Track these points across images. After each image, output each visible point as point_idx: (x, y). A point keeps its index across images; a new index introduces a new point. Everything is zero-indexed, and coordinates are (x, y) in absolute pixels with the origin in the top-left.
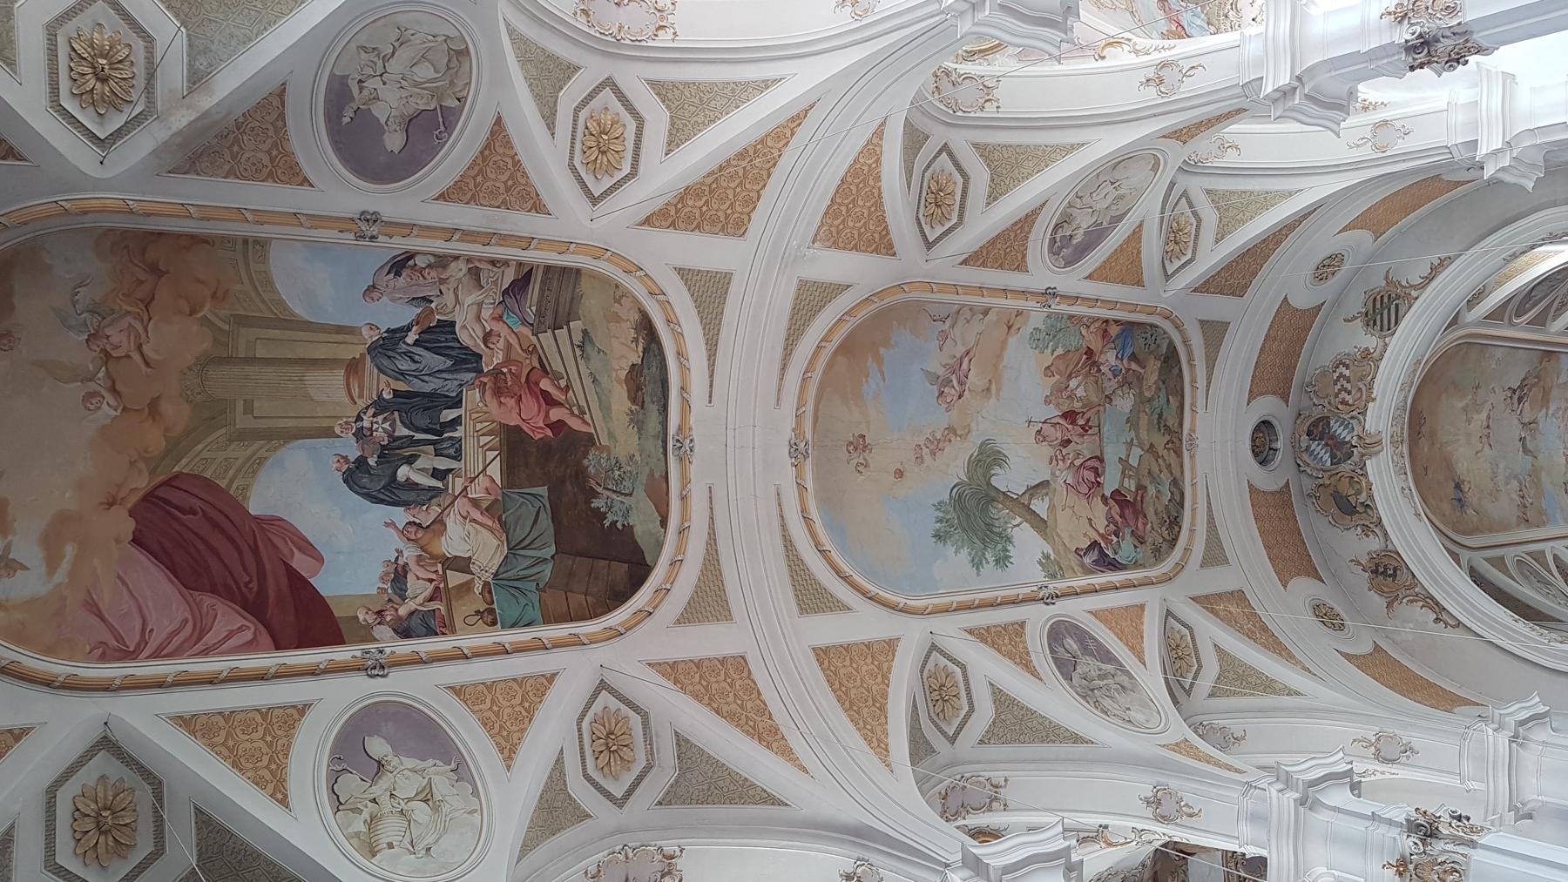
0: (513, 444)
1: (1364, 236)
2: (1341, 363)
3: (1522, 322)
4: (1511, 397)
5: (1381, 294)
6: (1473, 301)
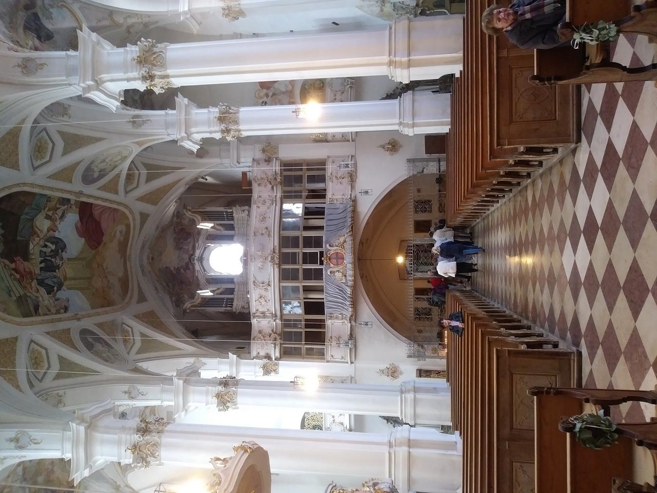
0: (26, 257)
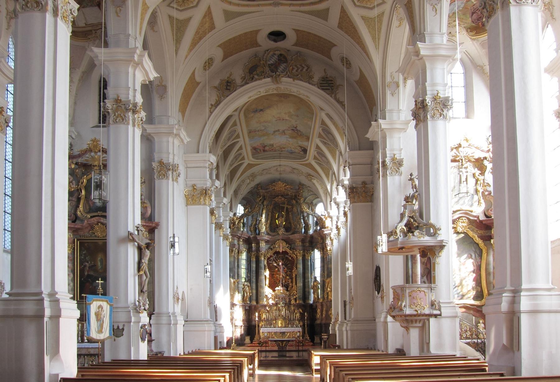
4: (293, 127)
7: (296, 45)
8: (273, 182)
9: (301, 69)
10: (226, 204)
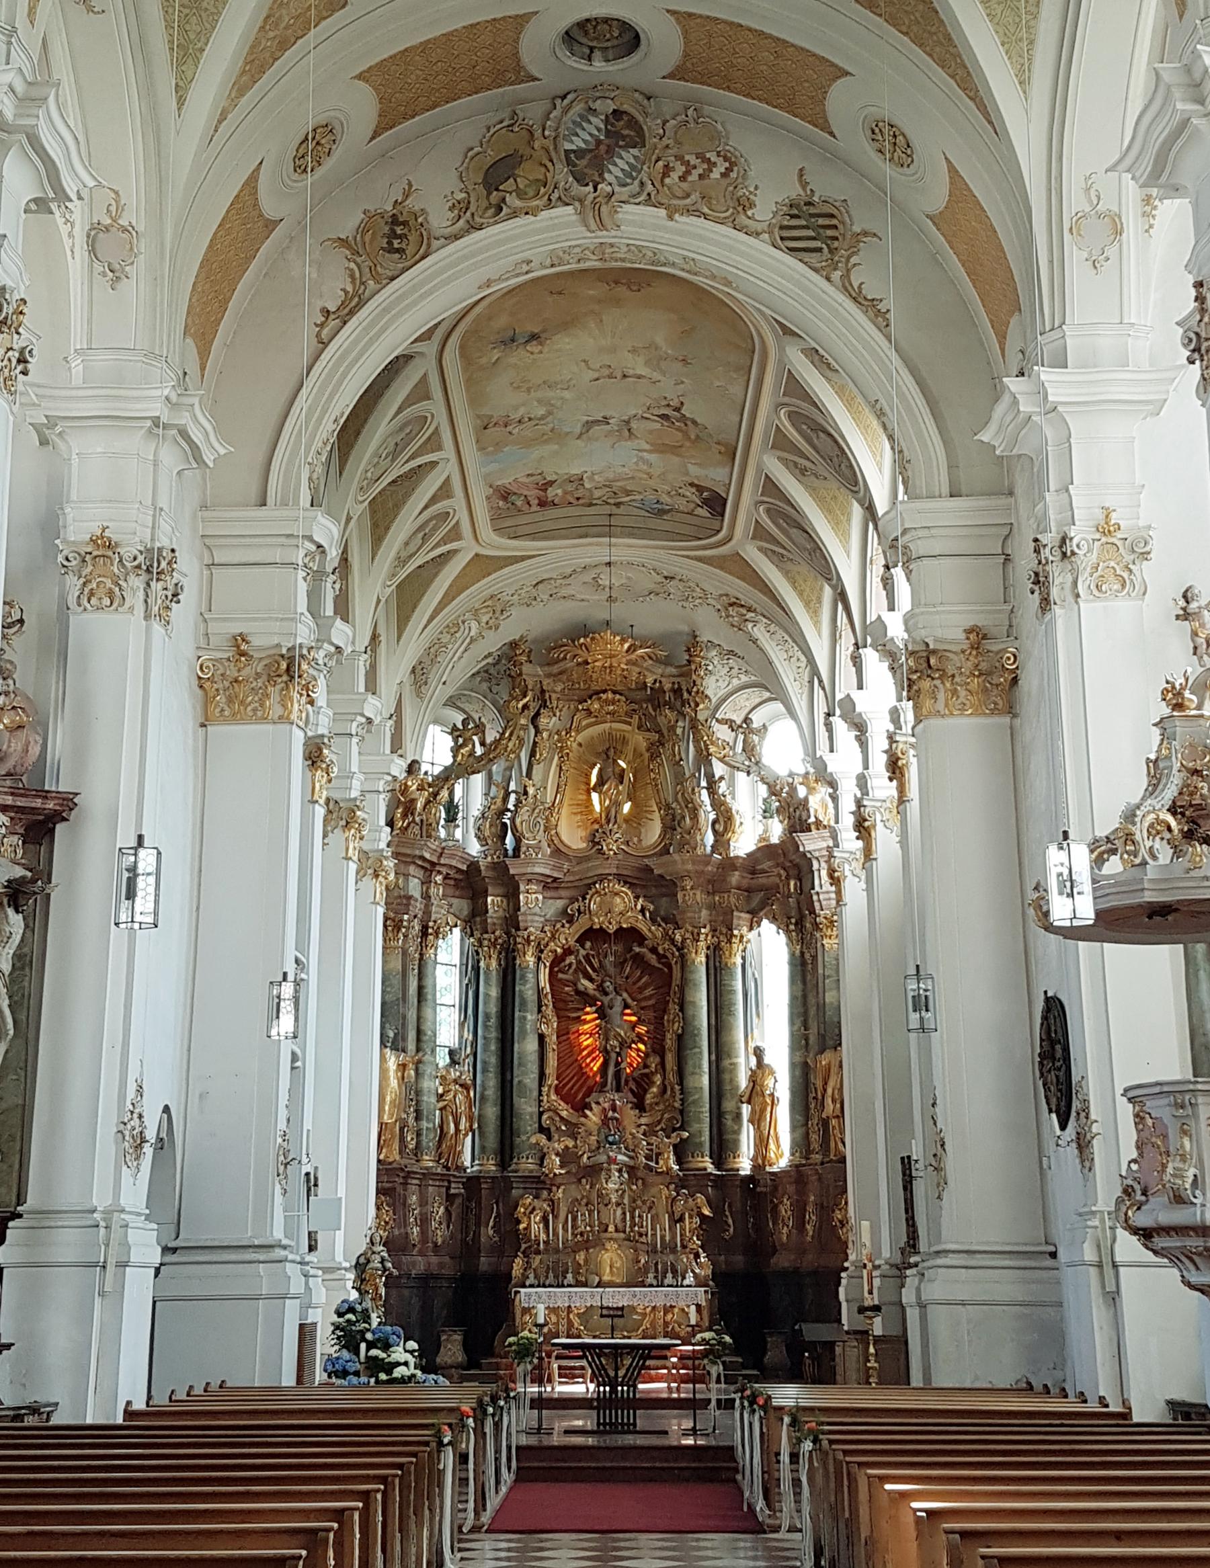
1: (937, 197)
2: (733, 164)
3: (779, 419)
4: (668, 405)
5: (840, 227)
6: (814, 355)
7: (678, 74)
8: (580, 633)
9: (701, 171)
10: (377, 721)
